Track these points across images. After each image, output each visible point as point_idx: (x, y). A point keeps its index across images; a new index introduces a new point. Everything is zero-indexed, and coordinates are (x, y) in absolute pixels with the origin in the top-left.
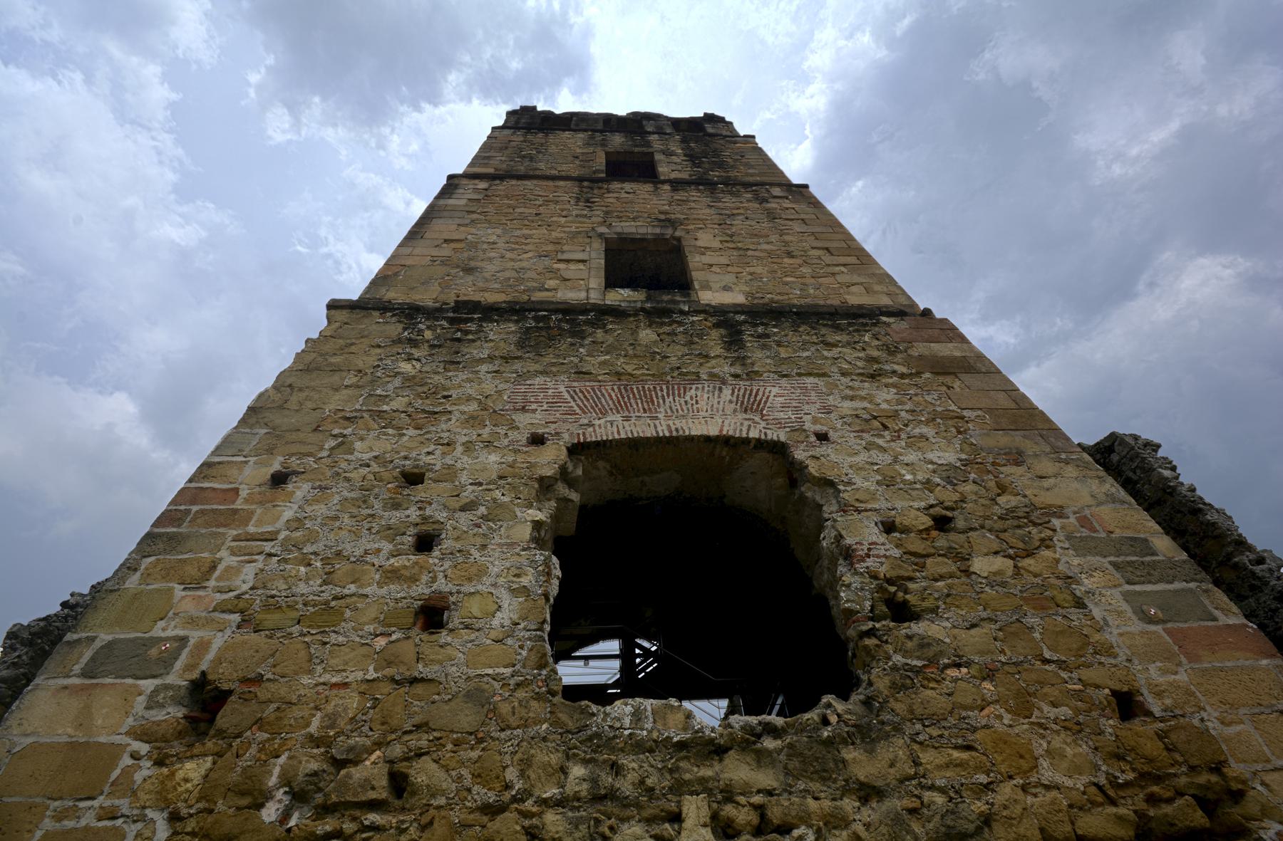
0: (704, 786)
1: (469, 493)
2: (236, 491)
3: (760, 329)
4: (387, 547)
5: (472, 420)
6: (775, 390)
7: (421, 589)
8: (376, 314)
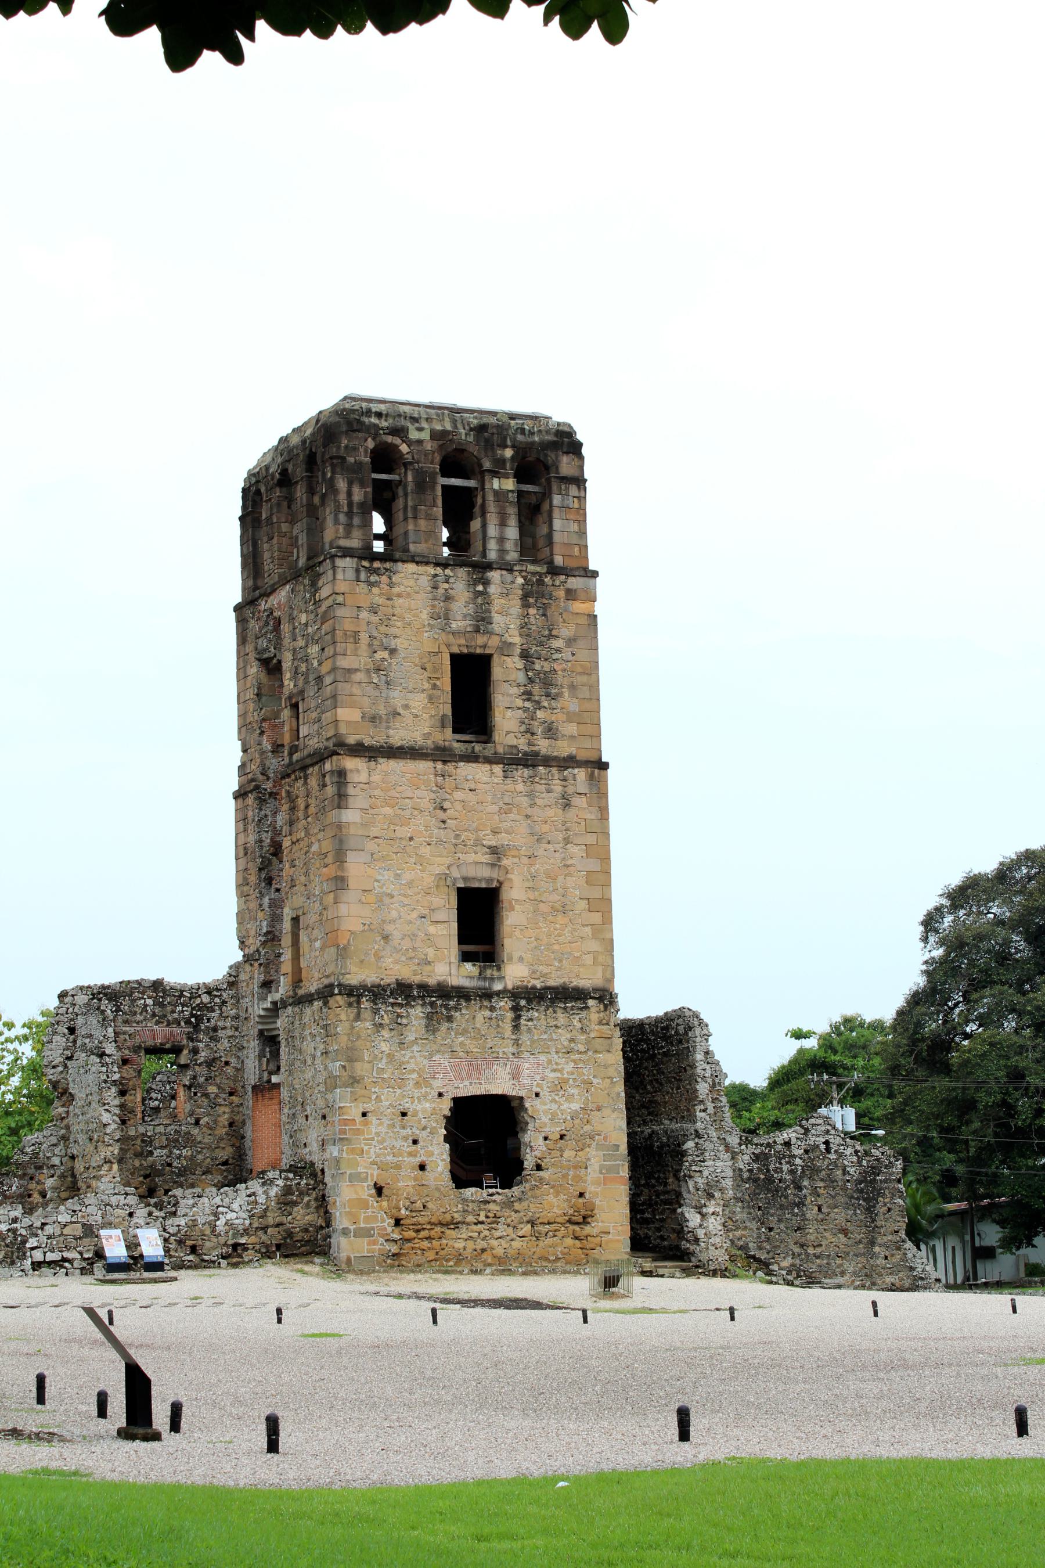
2: (354, 1120)
3: (529, 1014)
4: (406, 1144)
5: (417, 1084)
6: (527, 1065)
7: (417, 1160)
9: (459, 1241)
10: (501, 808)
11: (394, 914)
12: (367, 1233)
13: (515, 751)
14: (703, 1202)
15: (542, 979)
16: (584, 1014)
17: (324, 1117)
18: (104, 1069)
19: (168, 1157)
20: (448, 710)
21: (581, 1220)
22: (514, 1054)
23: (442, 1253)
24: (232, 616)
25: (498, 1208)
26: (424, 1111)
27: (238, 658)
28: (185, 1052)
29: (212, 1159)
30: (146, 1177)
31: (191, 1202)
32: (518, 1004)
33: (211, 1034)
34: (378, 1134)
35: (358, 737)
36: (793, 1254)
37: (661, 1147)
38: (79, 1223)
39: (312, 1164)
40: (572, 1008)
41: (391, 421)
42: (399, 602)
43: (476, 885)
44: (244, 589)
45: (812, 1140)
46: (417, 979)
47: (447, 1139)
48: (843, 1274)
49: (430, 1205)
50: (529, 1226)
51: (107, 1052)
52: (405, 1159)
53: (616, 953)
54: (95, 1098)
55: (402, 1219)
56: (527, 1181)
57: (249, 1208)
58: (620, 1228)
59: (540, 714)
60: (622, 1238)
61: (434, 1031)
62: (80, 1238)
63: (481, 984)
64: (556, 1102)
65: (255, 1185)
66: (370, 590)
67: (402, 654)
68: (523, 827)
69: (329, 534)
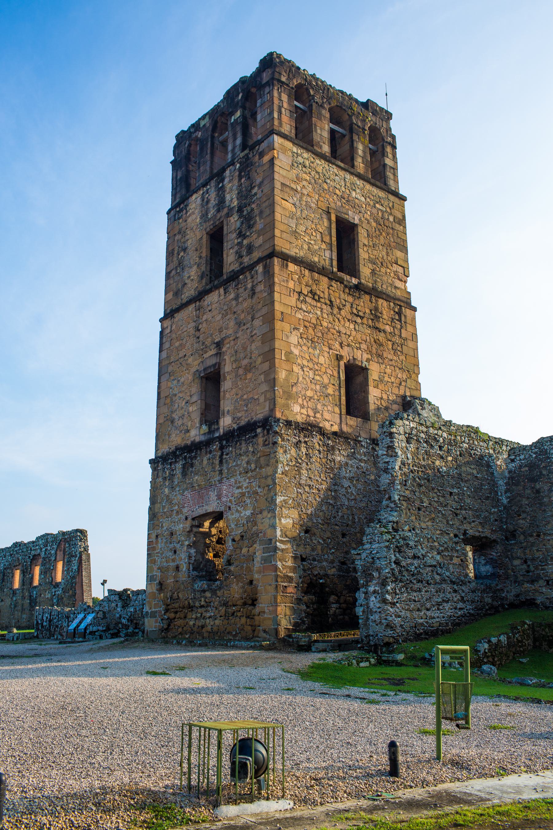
0: (203, 597)
5: (177, 512)
6: (225, 487)
7: (176, 564)
9: (193, 620)
12: (153, 615)
15: (238, 422)
16: (254, 440)
21: (250, 602)
35: (171, 308)
40: (249, 439)
50: (224, 608)
55: (168, 605)
59: (245, 242)
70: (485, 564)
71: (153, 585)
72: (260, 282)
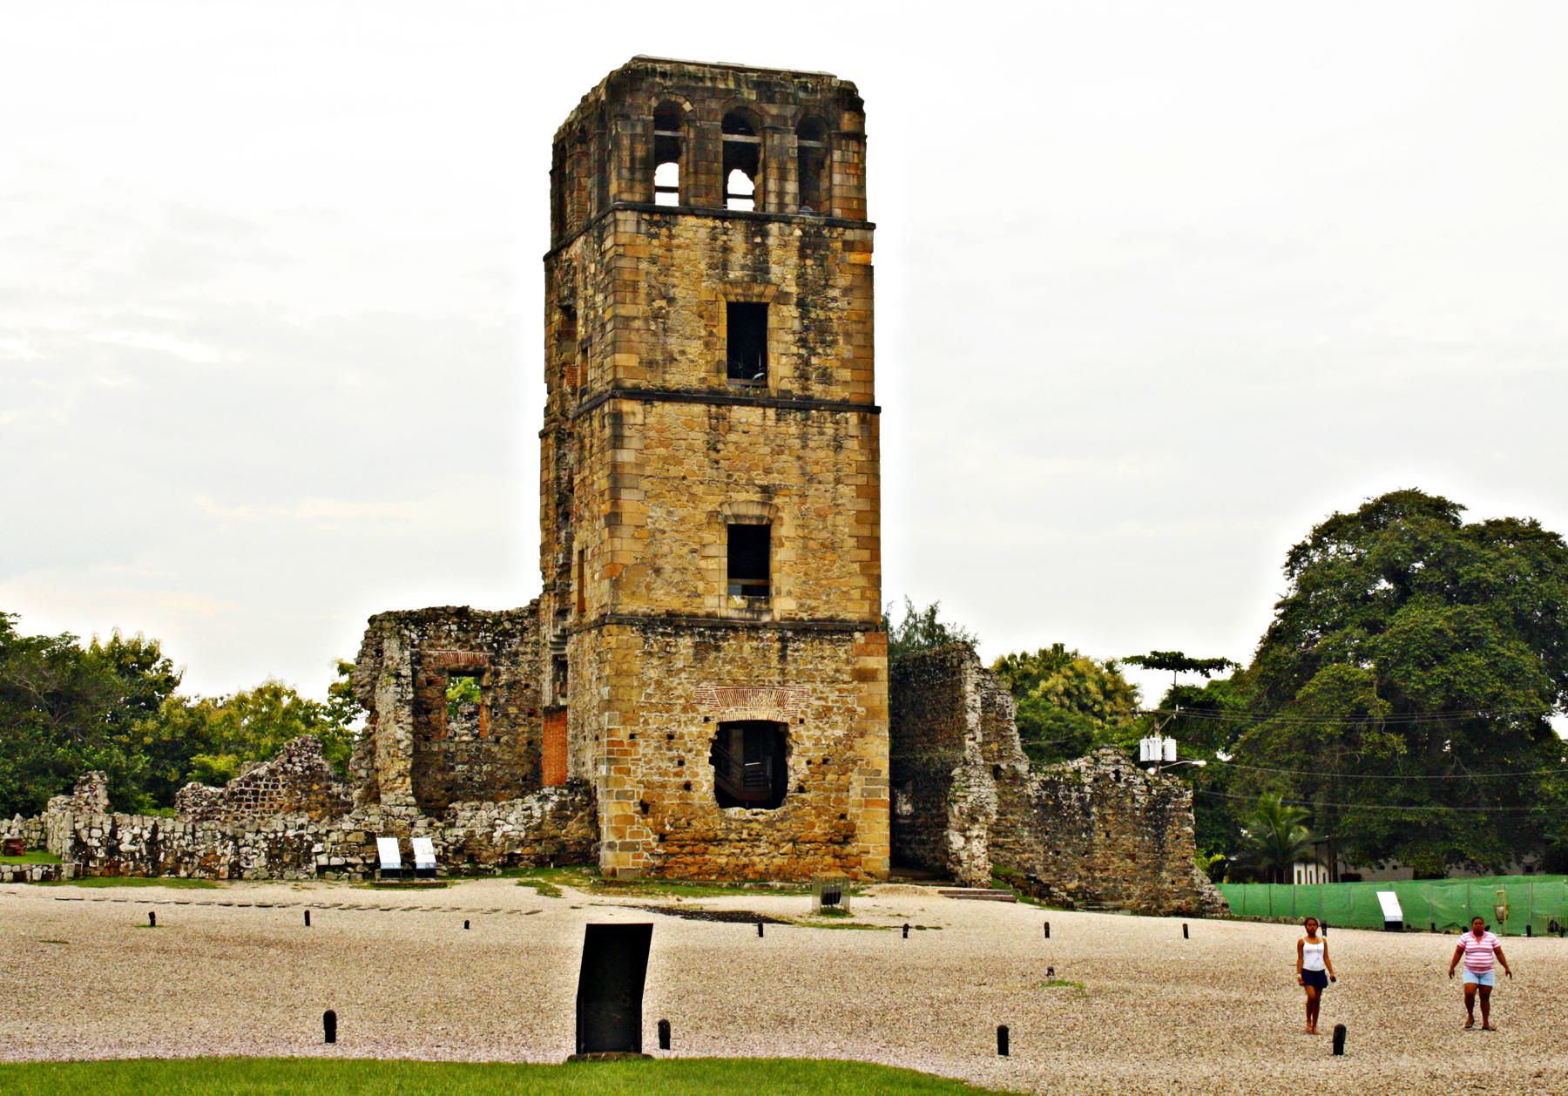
1: (690, 745)
3: (796, 645)
5: (685, 710)
6: (792, 693)
7: (683, 780)
8: (628, 628)
10: (773, 450)
11: (666, 549)
13: (788, 396)
14: (967, 825)
16: (848, 646)
17: (597, 738)
18: (399, 689)
19: (469, 772)
20: (722, 355)
22: (779, 683)
23: (704, 868)
24: (542, 264)
25: (760, 827)
26: (691, 734)
27: (546, 305)
28: (487, 675)
29: (511, 775)
30: (448, 790)
31: (469, 814)
32: (784, 636)
33: (513, 658)
34: (645, 755)
35: (635, 381)
36: (1080, 877)
37: (936, 773)
38: (361, 830)
39: (587, 782)
40: (838, 640)
41: (675, 80)
42: (677, 253)
43: (747, 522)
44: (553, 240)
45: (1102, 769)
46: (688, 610)
47: (712, 761)
48: (1129, 897)
49: (694, 823)
50: (791, 844)
51: (403, 673)
52: (671, 779)
53: (883, 589)
54: (392, 715)
56: (791, 802)
57: (525, 821)
58: (880, 849)
59: (814, 360)
60: (881, 858)
61: (702, 660)
62: (363, 845)
63: (748, 615)
64: (820, 728)
65: (531, 800)
66: (650, 242)
67: (680, 303)
68: (795, 471)
69: (613, 189)
70: (906, 804)
71: (625, 805)
72: (853, 437)
